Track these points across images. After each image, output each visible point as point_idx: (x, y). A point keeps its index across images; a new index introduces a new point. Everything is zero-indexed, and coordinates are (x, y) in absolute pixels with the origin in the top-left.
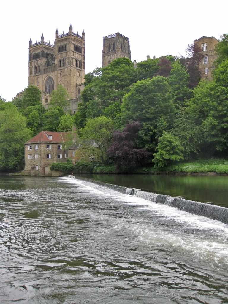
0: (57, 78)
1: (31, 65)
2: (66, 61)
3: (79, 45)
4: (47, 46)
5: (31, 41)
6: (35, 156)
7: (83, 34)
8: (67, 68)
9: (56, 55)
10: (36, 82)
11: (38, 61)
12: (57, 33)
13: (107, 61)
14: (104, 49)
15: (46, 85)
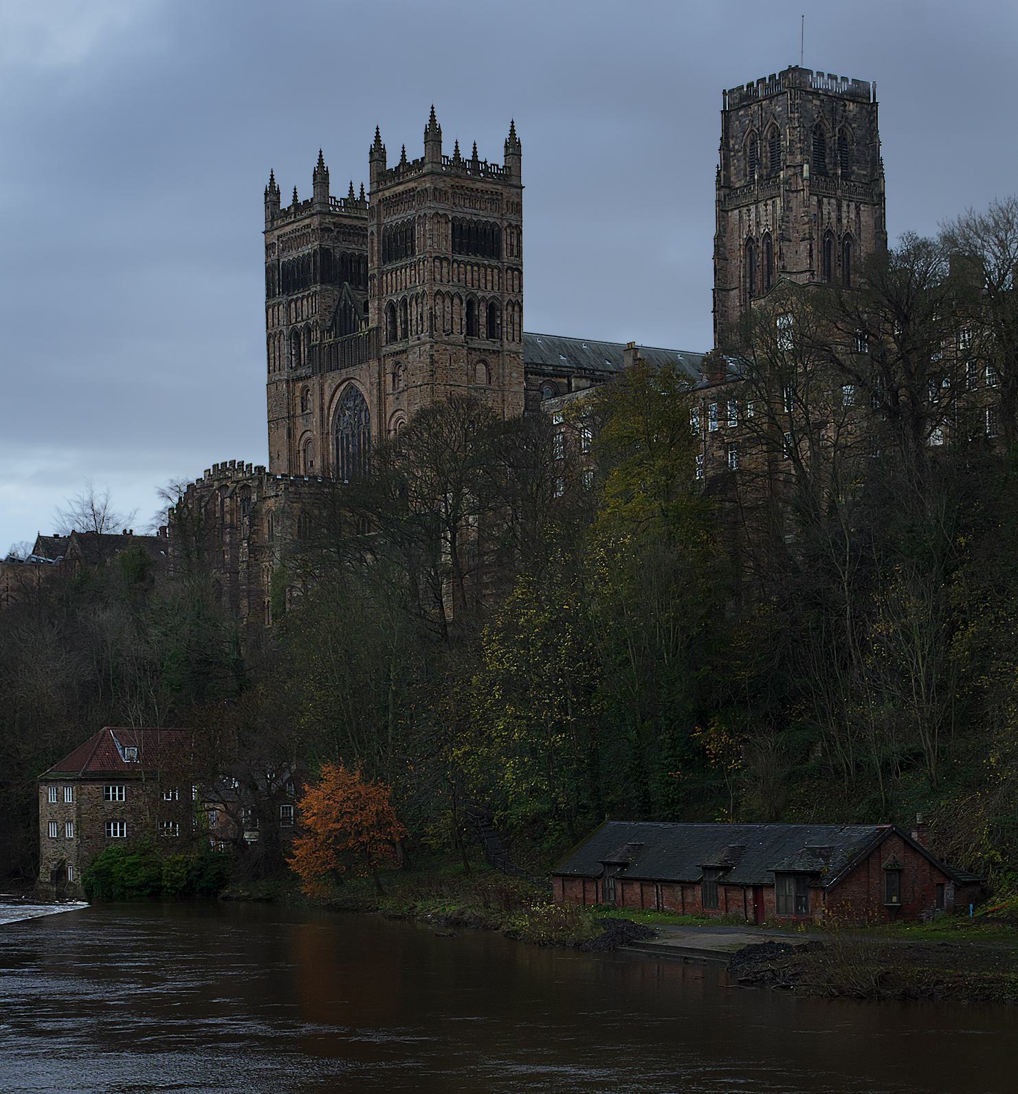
0: (381, 401)
1: (276, 321)
2: (414, 312)
3: (485, 215)
4: (346, 221)
5: (279, 193)
6: (64, 827)
7: (513, 147)
8: (417, 348)
9: (373, 276)
10: (299, 411)
11: (305, 302)
12: (378, 152)
13: (737, 242)
14: (725, 165)
15: (337, 432)
